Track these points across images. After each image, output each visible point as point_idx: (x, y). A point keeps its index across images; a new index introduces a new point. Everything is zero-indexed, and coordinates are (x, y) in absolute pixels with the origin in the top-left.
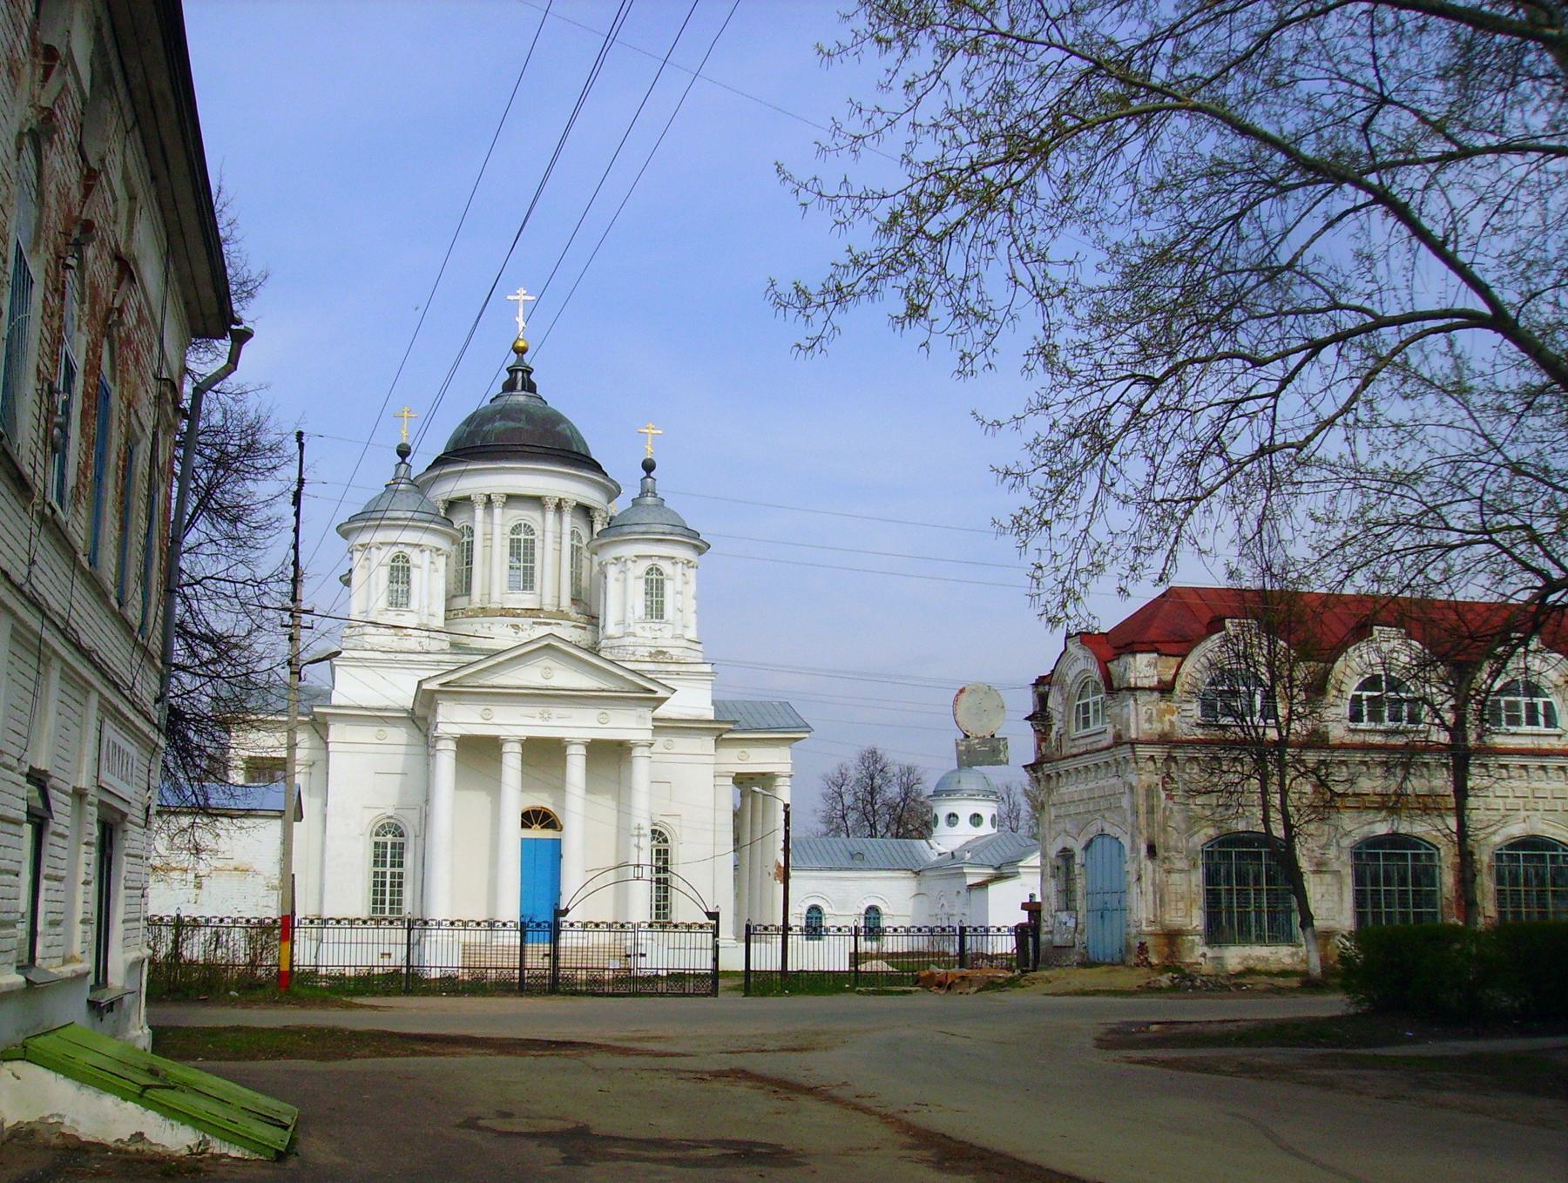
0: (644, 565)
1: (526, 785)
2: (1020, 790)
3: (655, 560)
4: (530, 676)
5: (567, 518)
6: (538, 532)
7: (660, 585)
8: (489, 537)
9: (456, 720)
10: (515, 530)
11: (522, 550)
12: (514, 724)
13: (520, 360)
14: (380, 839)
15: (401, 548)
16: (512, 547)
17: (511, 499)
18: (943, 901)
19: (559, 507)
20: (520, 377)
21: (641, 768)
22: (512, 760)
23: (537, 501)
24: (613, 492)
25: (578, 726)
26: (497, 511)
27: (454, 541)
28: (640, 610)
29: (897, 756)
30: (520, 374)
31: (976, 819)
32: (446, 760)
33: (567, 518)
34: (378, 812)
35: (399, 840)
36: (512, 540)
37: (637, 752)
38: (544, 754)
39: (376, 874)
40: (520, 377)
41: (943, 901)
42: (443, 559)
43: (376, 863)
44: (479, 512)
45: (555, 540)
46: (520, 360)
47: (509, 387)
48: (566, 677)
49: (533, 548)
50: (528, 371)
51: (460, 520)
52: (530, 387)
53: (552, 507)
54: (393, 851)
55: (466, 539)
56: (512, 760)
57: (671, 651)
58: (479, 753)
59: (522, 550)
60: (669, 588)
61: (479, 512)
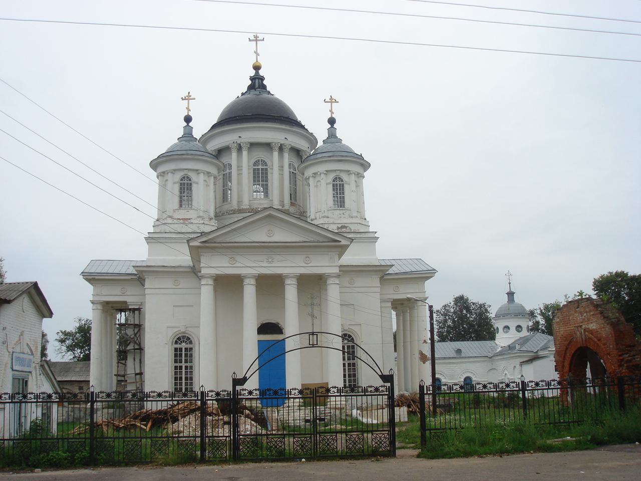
0: (332, 176)
1: (260, 306)
2: (539, 311)
3: (338, 173)
4: (260, 235)
5: (286, 155)
6: (269, 164)
7: (342, 187)
8: (239, 168)
9: (216, 265)
10: (255, 164)
11: (260, 176)
12: (249, 267)
13: (257, 73)
14: (178, 346)
15: (186, 172)
16: (254, 173)
17: (253, 145)
18: (506, 372)
19: (281, 149)
20: (257, 83)
21: (333, 291)
22: (250, 291)
23: (268, 146)
24: (312, 140)
25: (291, 266)
26: (245, 153)
27: (219, 170)
28: (331, 202)
29: (475, 297)
30: (257, 81)
31: (519, 328)
32: (207, 291)
33: (286, 155)
34: (176, 330)
35: (189, 346)
36: (254, 170)
37: (330, 281)
38: (271, 286)
39: (176, 368)
40: (257, 83)
41: (506, 372)
43: (176, 361)
44: (234, 155)
45: (279, 168)
46: (257, 73)
47: (251, 88)
48: (281, 236)
49: (267, 174)
51: (225, 159)
52: (264, 87)
53: (277, 149)
54: (183, 351)
55: (228, 171)
56: (250, 291)
57: (350, 226)
58: (228, 286)
59: (260, 176)
60: (347, 188)
61: (234, 155)
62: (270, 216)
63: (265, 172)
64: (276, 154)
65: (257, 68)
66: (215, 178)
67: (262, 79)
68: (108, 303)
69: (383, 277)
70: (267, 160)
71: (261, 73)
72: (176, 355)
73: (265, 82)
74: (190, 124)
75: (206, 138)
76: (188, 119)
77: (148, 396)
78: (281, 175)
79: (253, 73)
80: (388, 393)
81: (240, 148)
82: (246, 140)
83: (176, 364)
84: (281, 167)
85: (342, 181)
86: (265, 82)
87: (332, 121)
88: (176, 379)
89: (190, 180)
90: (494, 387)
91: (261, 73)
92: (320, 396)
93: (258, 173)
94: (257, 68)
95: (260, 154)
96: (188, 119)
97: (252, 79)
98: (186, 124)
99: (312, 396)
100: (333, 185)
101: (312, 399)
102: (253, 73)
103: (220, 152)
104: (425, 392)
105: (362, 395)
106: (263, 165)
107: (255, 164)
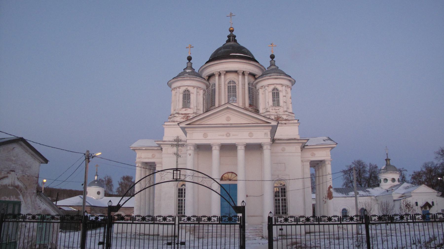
6: (237, 83)
7: (278, 94)
10: (229, 83)
17: (227, 72)
19: (243, 74)
20: (232, 38)
26: (223, 77)
28: (271, 103)
30: (231, 37)
31: (393, 180)
33: (246, 77)
36: (228, 86)
39: (179, 200)
40: (232, 38)
42: (202, 91)
43: (179, 197)
44: (217, 78)
47: (228, 41)
49: (235, 88)
50: (235, 37)
51: (212, 81)
52: (235, 41)
53: (241, 74)
60: (281, 95)
61: (217, 78)
62: (228, 108)
63: (234, 88)
64: (240, 77)
65: (231, 31)
66: (204, 90)
67: (235, 37)
68: (146, 163)
69: (304, 147)
70: (235, 81)
71: (234, 33)
72: (179, 193)
73: (236, 38)
74: (191, 61)
76: (189, 59)
78: (244, 88)
79: (229, 33)
80: (239, 222)
81: (220, 75)
82: (224, 70)
83: (179, 198)
84: (244, 85)
85: (278, 90)
86: (236, 38)
87: (272, 57)
88: (179, 207)
89: (189, 92)
90: (295, 220)
91: (234, 33)
92: (182, 224)
93: (231, 89)
94: (231, 31)
95: (231, 77)
96: (189, 59)
97: (229, 37)
98: (188, 61)
99: (174, 222)
100: (273, 93)
101: (173, 226)
102: (229, 33)
104: (274, 223)
105: (217, 224)
106: (233, 84)
107: (229, 83)
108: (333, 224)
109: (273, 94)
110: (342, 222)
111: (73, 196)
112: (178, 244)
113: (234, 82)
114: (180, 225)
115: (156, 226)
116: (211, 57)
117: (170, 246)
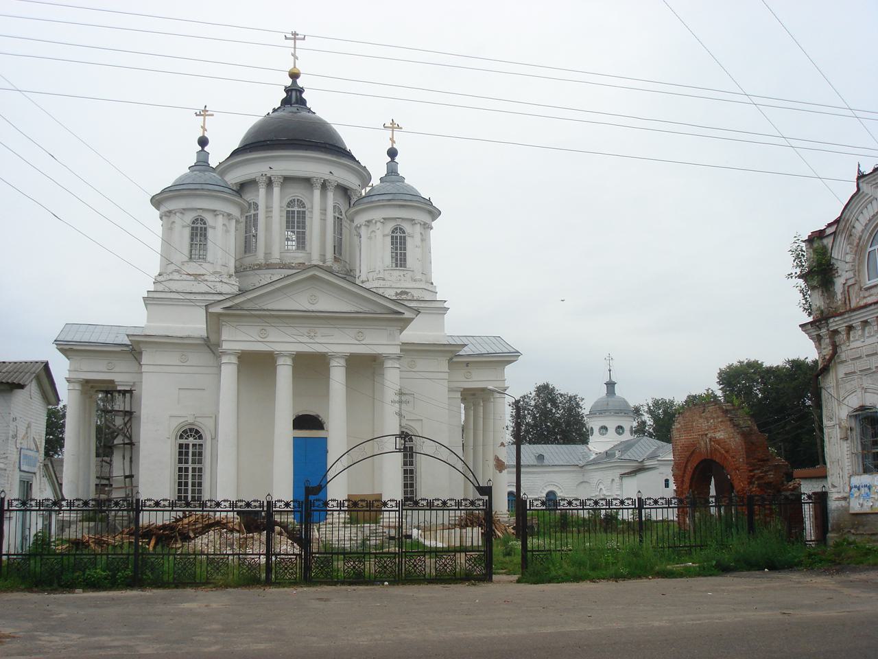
0: (390, 226)
1: (297, 393)
2: (646, 408)
3: (399, 222)
4: (300, 302)
5: (330, 195)
6: (308, 205)
8: (269, 209)
9: (238, 339)
10: (290, 204)
11: (296, 220)
12: (285, 342)
13: (294, 82)
14: (183, 441)
15: (200, 213)
16: (288, 217)
17: (287, 180)
18: (601, 486)
19: (324, 186)
20: (294, 96)
21: (392, 377)
22: (284, 372)
23: (307, 181)
24: (364, 176)
25: (338, 343)
26: (276, 190)
27: (242, 211)
29: (563, 387)
30: (294, 93)
31: (620, 429)
32: (229, 372)
33: (330, 195)
34: (182, 420)
35: (198, 442)
36: (288, 212)
37: (388, 364)
38: (311, 367)
39: (180, 470)
40: (294, 96)
41: (601, 486)
42: (233, 222)
43: (180, 461)
44: (262, 191)
45: (321, 211)
46: (294, 82)
47: (285, 102)
48: (327, 303)
49: (304, 218)
50: (301, 91)
51: (249, 196)
52: (303, 102)
53: (319, 186)
54: (191, 447)
55: (253, 212)
56: (284, 372)
57: (412, 292)
58: (256, 365)
59: (296, 220)
61: (262, 191)
62: (314, 278)
63: (302, 215)
64: (317, 193)
65: (294, 76)
66: (237, 222)
67: (301, 91)
68: (87, 382)
69: (451, 359)
70: (305, 201)
71: (301, 82)
72: (180, 453)
73: (304, 96)
74: (206, 149)
75: (226, 167)
76: (203, 142)
77: (385, 504)
78: (324, 220)
79: (289, 82)
80: (485, 508)
81: (270, 183)
82: (279, 173)
83: (181, 465)
84: (324, 211)
85: (404, 232)
86: (304, 96)
87: (392, 153)
88: (180, 484)
89: (205, 223)
91: (301, 82)
92: (406, 510)
93: (293, 217)
94: (294, 76)
95: (296, 192)
96: (203, 142)
97: (287, 90)
98: (200, 148)
99: (398, 509)
100: (392, 237)
101: (397, 513)
102: (289, 82)
103: (242, 187)
104: (528, 508)
105: (455, 510)
106: (299, 207)
107: (289, 205)
108: (628, 509)
109: (394, 240)
110: (611, 507)
111: (295, 475)
112: (399, 539)
113: (302, 204)
114: (404, 512)
115: (434, 512)
116: (246, 138)
117: (394, 541)
